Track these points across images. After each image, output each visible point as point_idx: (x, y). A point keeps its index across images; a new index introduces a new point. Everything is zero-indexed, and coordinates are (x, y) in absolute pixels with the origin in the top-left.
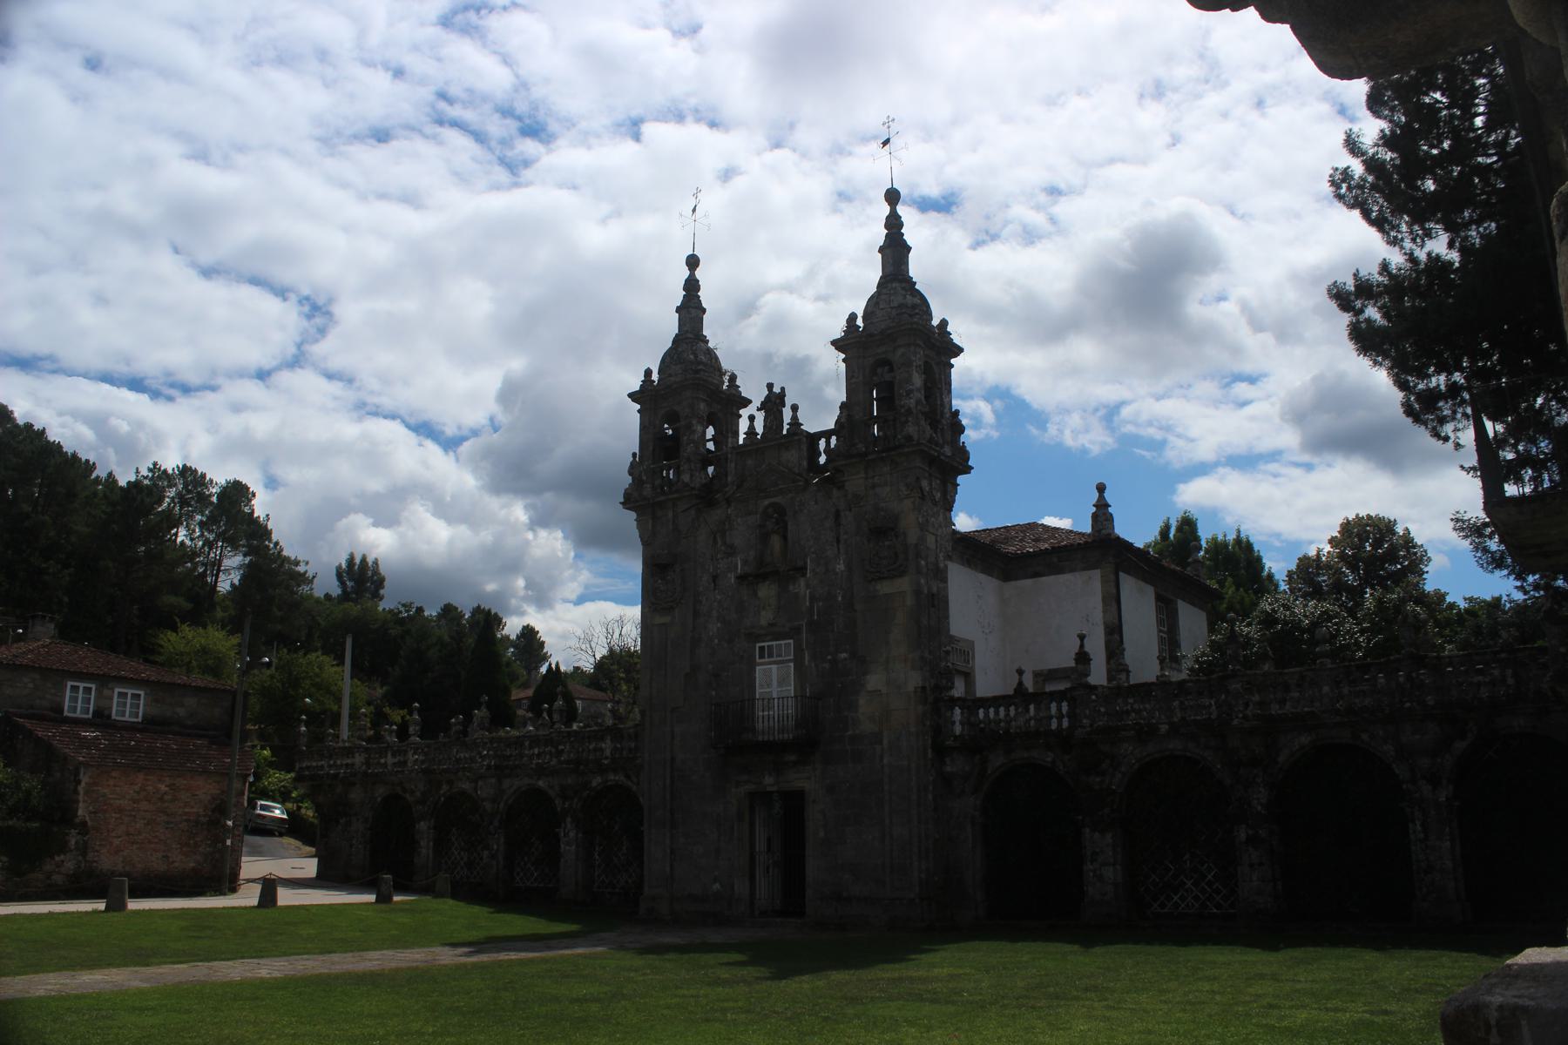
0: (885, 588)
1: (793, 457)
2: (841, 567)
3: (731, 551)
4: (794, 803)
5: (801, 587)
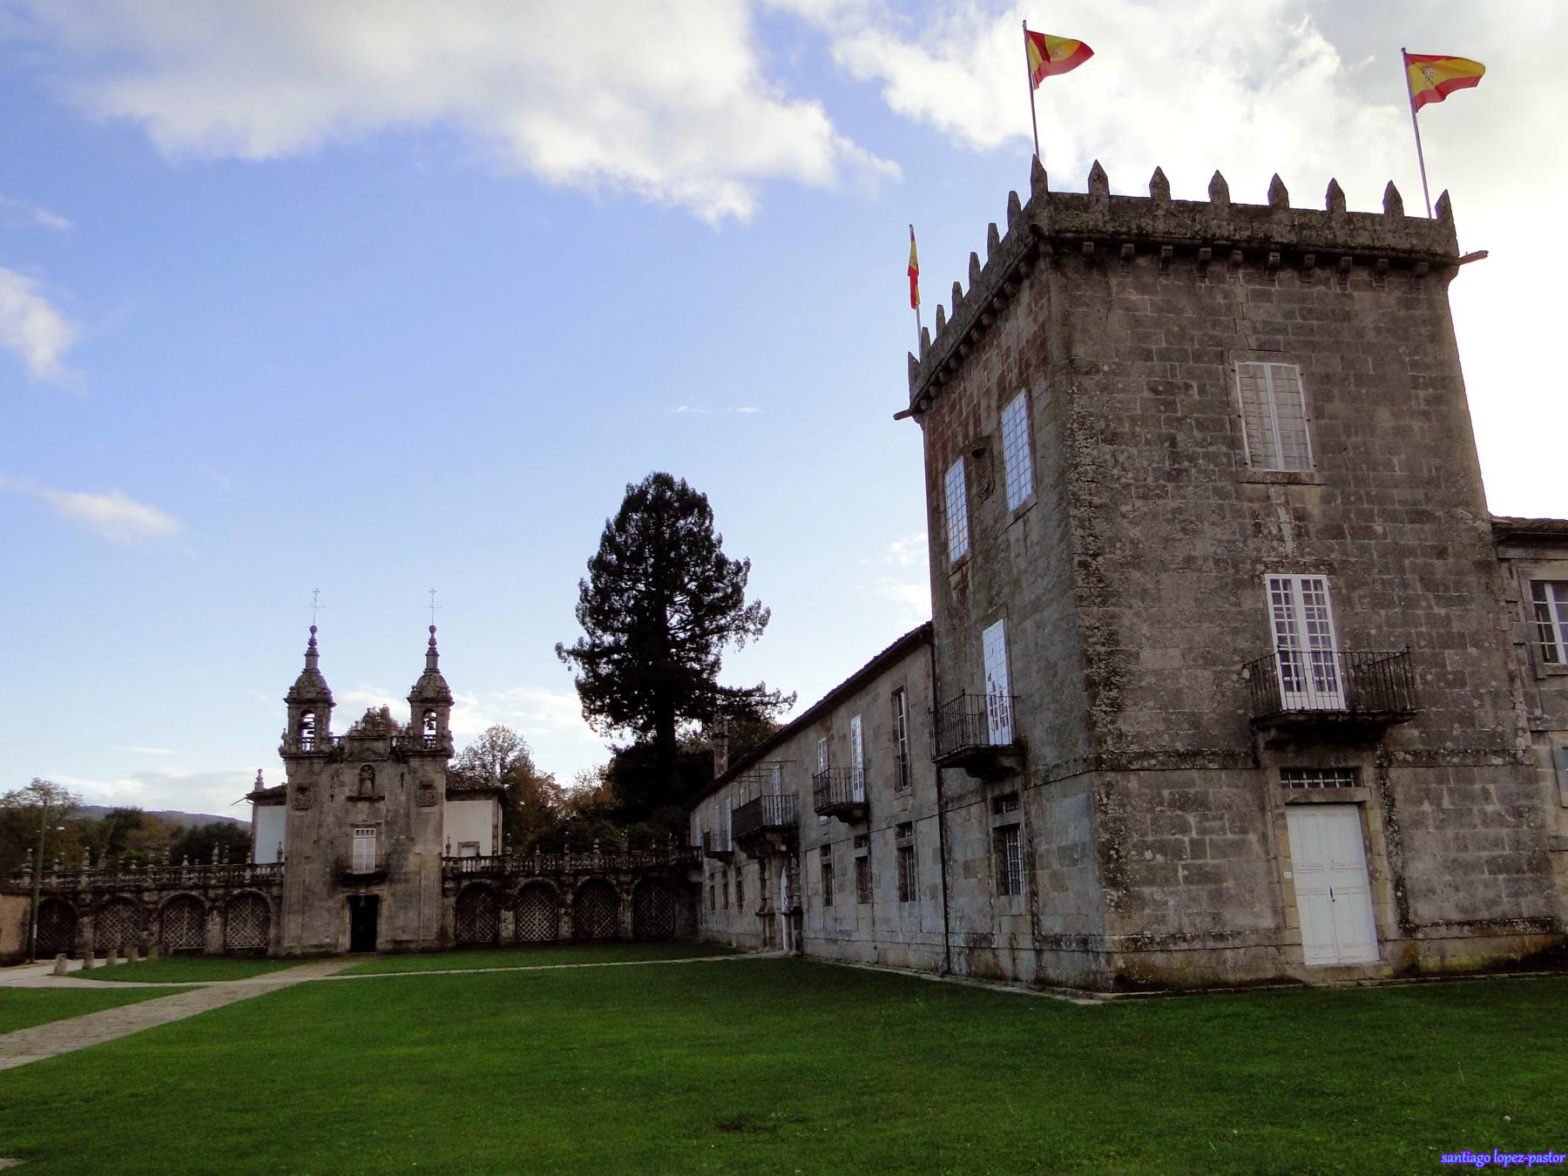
0: (426, 810)
1: (380, 746)
2: (403, 798)
3: (342, 784)
4: (375, 901)
5: (381, 805)
